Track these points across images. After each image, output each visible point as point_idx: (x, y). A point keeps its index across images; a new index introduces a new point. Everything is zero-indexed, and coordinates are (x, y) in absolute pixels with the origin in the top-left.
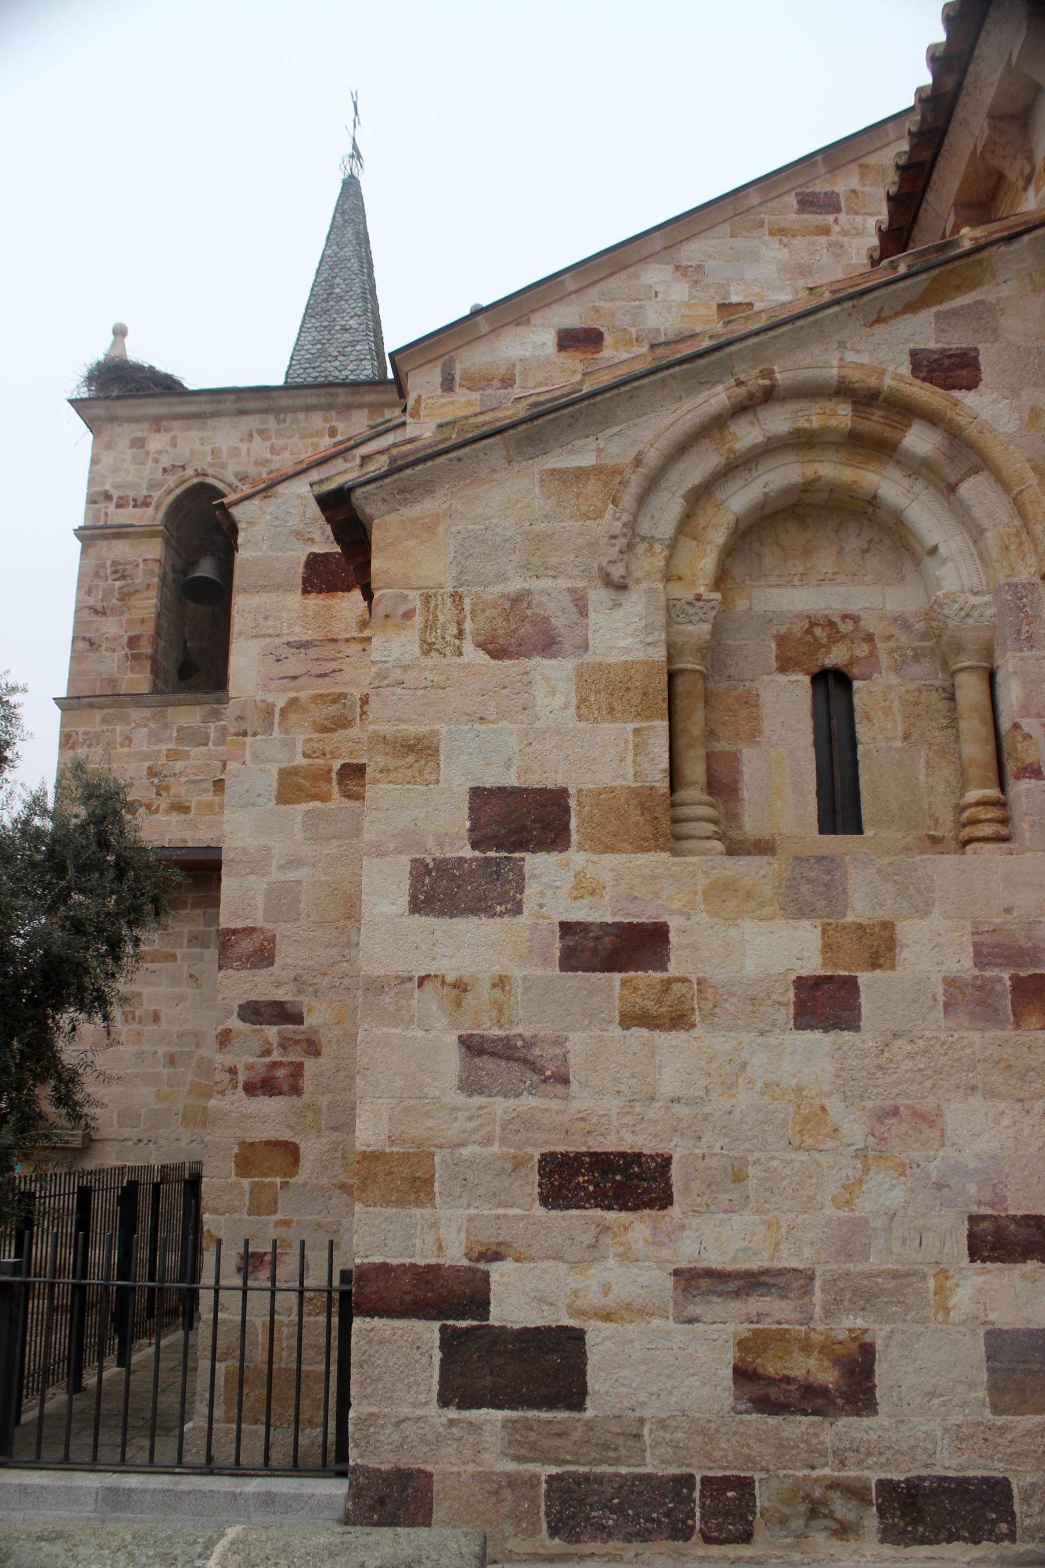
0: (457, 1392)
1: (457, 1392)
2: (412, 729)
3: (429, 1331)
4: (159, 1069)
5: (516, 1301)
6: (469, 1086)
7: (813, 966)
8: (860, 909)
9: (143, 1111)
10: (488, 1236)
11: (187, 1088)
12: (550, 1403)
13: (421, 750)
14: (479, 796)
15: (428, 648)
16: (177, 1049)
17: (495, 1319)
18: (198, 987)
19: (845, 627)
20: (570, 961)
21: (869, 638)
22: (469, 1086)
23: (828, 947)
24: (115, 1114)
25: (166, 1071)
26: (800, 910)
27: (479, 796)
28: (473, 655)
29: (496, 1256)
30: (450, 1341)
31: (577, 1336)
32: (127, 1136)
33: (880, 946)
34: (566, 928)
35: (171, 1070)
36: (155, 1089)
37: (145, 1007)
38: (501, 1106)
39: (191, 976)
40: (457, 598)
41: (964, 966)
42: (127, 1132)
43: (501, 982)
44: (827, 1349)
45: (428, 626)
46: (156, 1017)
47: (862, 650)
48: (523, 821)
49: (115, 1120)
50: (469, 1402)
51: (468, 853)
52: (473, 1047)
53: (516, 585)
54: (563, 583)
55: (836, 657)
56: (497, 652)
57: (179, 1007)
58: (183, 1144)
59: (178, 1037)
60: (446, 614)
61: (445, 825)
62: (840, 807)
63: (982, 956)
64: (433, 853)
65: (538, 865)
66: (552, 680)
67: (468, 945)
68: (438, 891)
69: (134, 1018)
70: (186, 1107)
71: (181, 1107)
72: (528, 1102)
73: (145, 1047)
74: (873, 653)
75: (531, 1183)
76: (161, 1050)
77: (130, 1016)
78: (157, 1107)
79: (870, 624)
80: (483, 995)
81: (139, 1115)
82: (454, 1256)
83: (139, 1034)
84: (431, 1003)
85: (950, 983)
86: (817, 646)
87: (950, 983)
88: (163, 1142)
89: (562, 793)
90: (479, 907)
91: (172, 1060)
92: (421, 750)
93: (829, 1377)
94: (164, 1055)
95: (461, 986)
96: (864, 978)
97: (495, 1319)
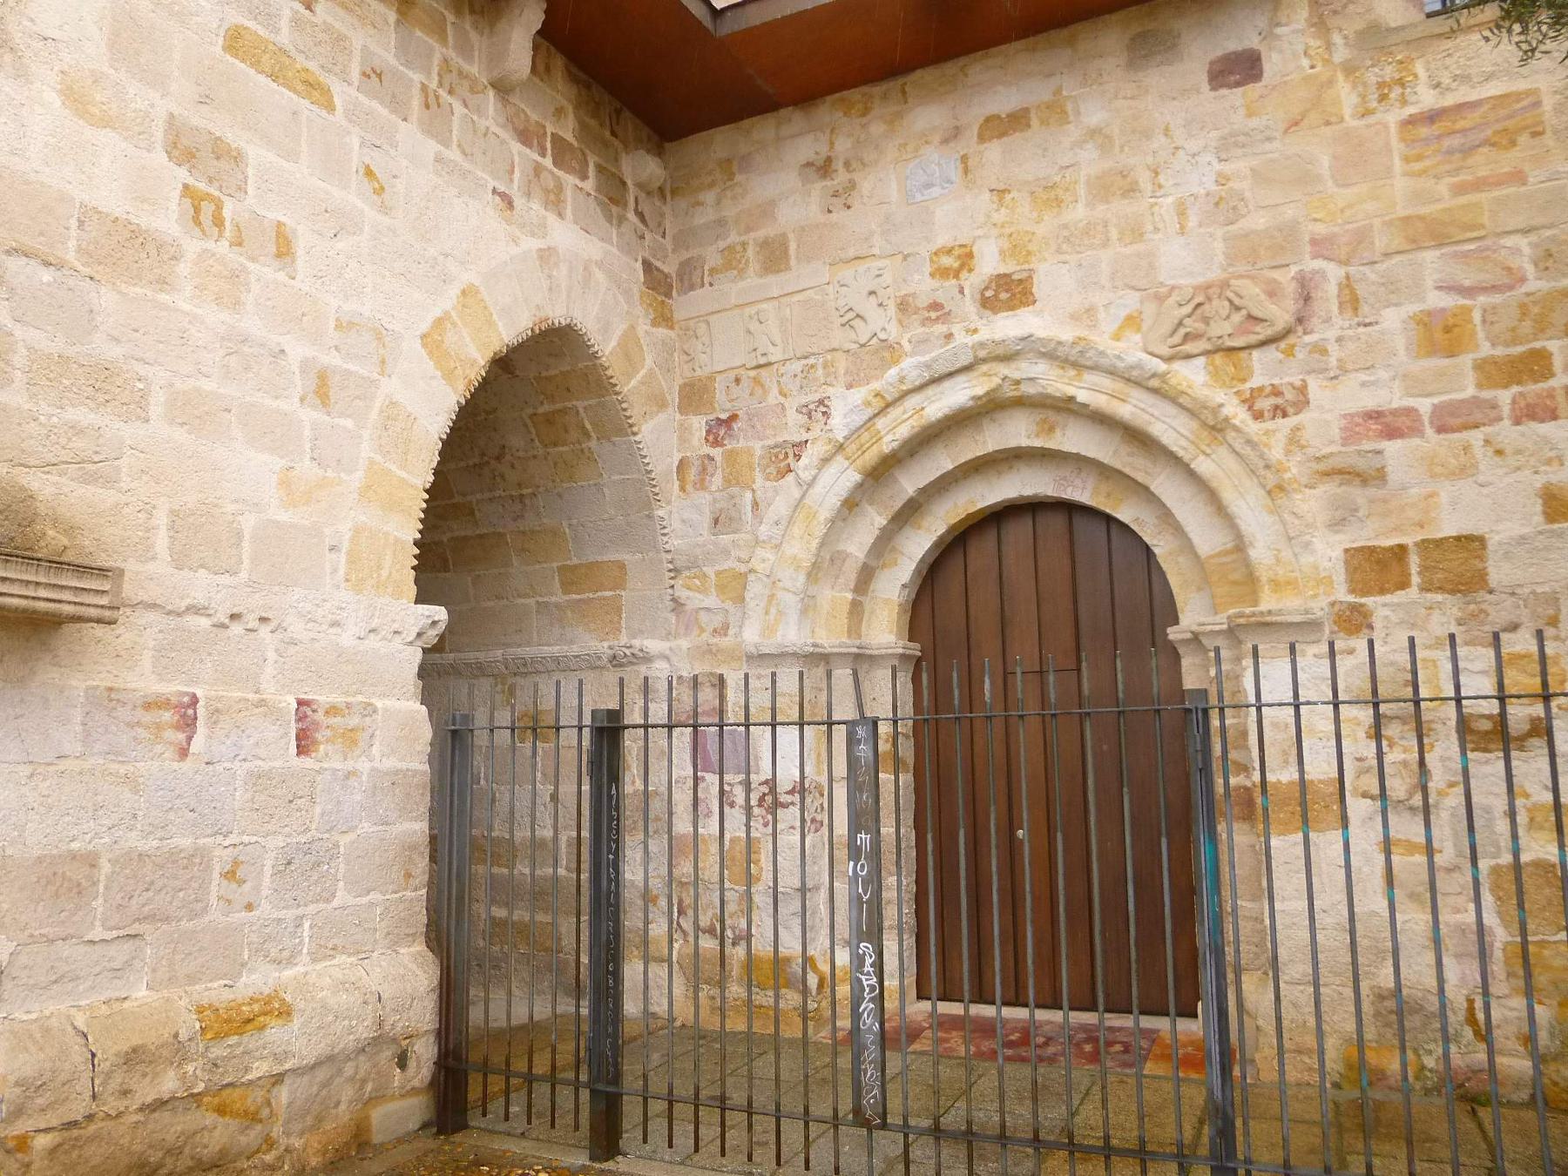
4: (290, 405)
9: (248, 523)
11: (357, 478)
16: (333, 360)
18: (384, 209)
24: (162, 519)
25: (309, 415)
32: (199, 598)
35: (318, 415)
36: (279, 463)
37: (251, 201)
39: (369, 173)
42: (200, 586)
46: (284, 248)
49: (161, 541)
57: (340, 245)
58: (347, 639)
59: (339, 326)
69: (218, 222)
70: (357, 531)
71: (345, 528)
73: (252, 324)
76: (297, 351)
77: (207, 209)
78: (283, 516)
81: (239, 535)
83: (236, 276)
88: (296, 628)
91: (322, 389)
94: (305, 365)
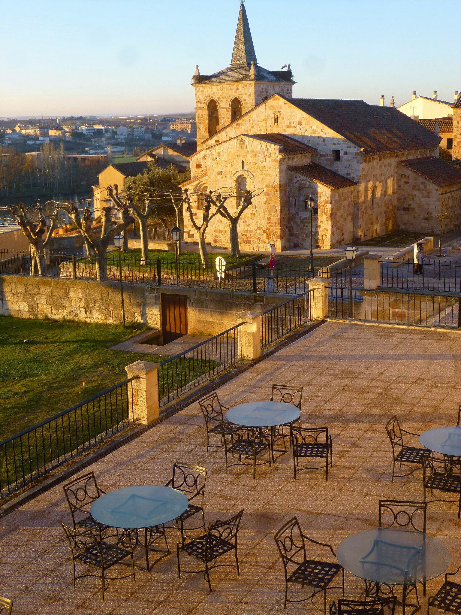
5: (191, 233)
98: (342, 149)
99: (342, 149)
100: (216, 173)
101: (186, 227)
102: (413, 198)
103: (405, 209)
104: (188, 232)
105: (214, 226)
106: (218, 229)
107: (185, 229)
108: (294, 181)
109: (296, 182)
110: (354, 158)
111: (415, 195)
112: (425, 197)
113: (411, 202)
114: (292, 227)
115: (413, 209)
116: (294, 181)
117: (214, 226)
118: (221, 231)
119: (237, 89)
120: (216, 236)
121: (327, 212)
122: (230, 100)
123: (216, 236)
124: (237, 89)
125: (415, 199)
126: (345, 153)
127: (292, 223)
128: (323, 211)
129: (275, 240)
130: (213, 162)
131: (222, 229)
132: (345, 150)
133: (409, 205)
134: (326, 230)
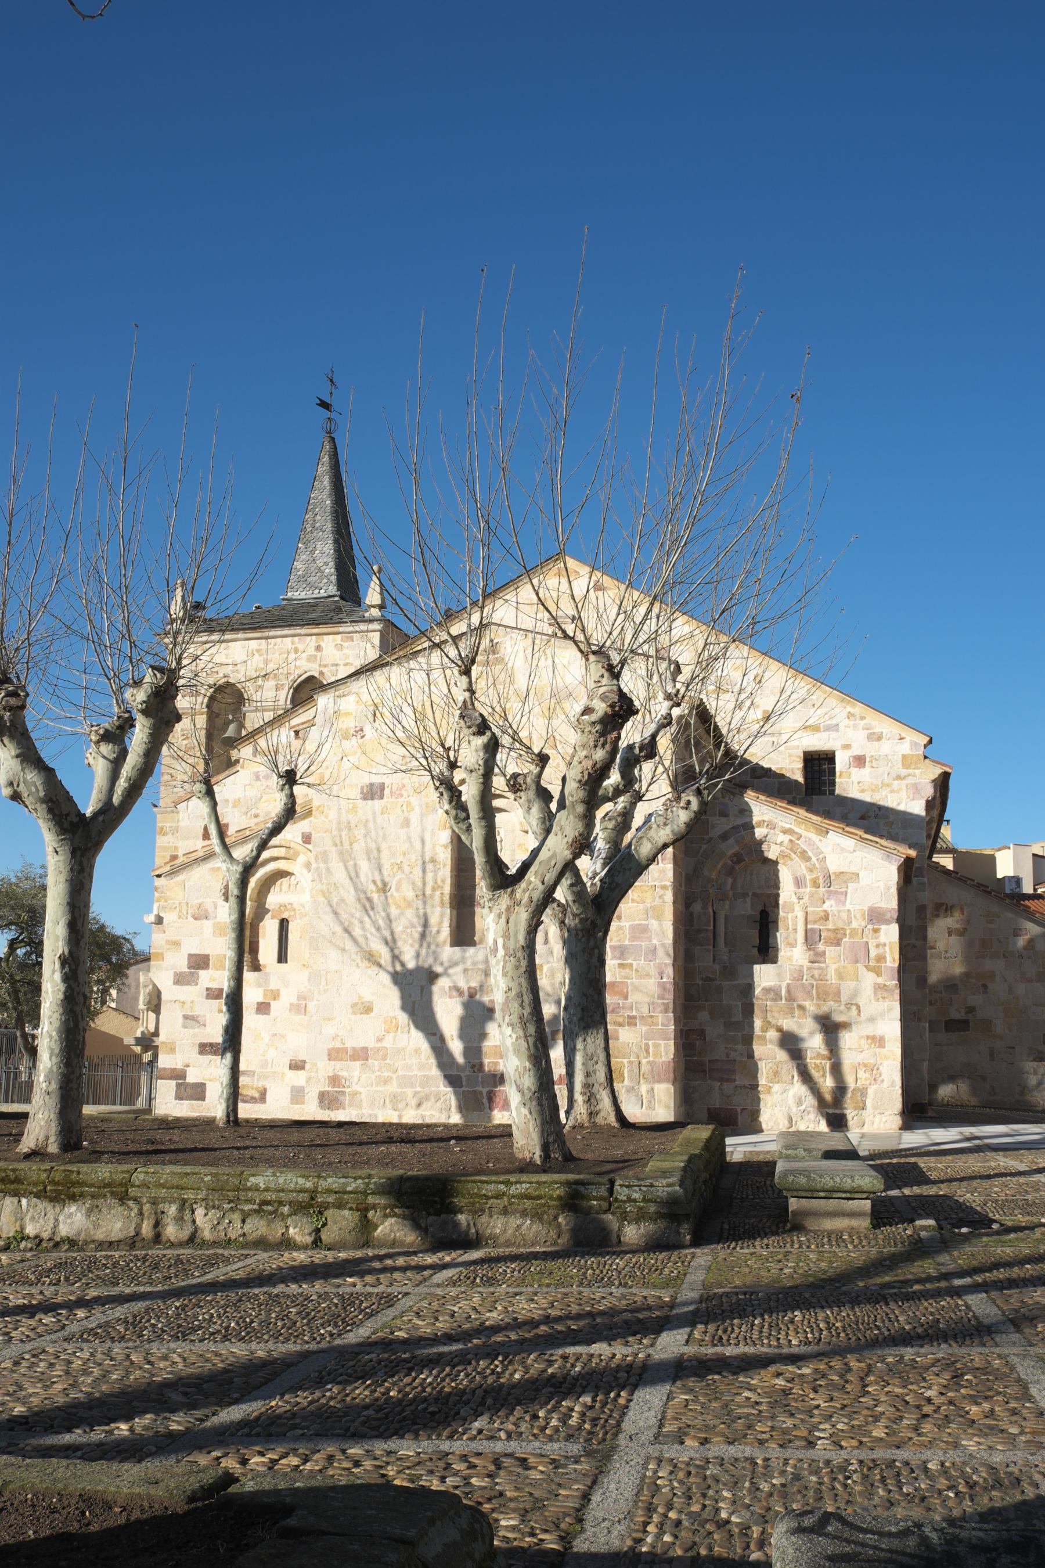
0: (179, 1097)
1: (179, 1097)
2: (175, 938)
3: (173, 1083)
5: (191, 1078)
6: (185, 1026)
7: (261, 1000)
8: (272, 986)
10: (186, 1061)
12: (198, 1099)
13: (177, 944)
14: (190, 956)
15: (180, 917)
17: (187, 1080)
19: (289, 907)
20: (208, 997)
21: (294, 910)
22: (185, 1026)
23: (265, 995)
26: (259, 985)
27: (190, 956)
28: (191, 919)
29: (188, 1066)
30: (178, 1085)
31: (205, 1084)
33: (276, 995)
34: (208, 989)
38: (191, 1031)
40: (187, 904)
41: (295, 1001)
43: (192, 1002)
44: (257, 1089)
45: (180, 911)
47: (292, 913)
48: (200, 962)
50: (181, 1099)
51: (187, 970)
52: (186, 1017)
53: (200, 901)
54: (212, 900)
55: (284, 916)
56: (196, 919)
60: (184, 907)
61: (182, 965)
62: (282, 958)
63: (299, 998)
64: (179, 970)
65: (201, 973)
66: (207, 925)
67: (186, 993)
68: (180, 979)
72: (197, 1030)
74: (295, 915)
75: (196, 1049)
79: (295, 906)
80: (188, 1005)
82: (179, 1066)
84: (177, 1006)
85: (291, 1004)
86: (281, 912)
87: (291, 1004)
89: (208, 956)
90: (188, 984)
92: (177, 944)
93: (257, 1095)
95: (183, 1003)
96: (272, 1003)
97: (187, 1080)
98: (847, 747)
99: (847, 747)
100: (355, 793)
101: (172, 1050)
102: (985, 986)
103: (963, 1025)
104: (178, 1075)
105: (330, 1030)
106: (349, 1044)
107: (164, 1061)
108: (715, 833)
109: (724, 837)
110: (899, 778)
111: (992, 976)
112: (1030, 981)
113: (976, 1000)
114: (702, 1033)
115: (987, 1025)
116: (715, 833)
117: (330, 1030)
118: (361, 1055)
119: (318, 648)
120: (334, 1080)
121: (881, 958)
122: (287, 683)
123: (334, 1080)
124: (318, 648)
125: (991, 986)
126: (860, 761)
127: (704, 1016)
128: (862, 954)
129: (644, 1089)
130: (346, 744)
131: (371, 1044)
132: (856, 751)
133: (971, 1010)
134: (879, 1041)
